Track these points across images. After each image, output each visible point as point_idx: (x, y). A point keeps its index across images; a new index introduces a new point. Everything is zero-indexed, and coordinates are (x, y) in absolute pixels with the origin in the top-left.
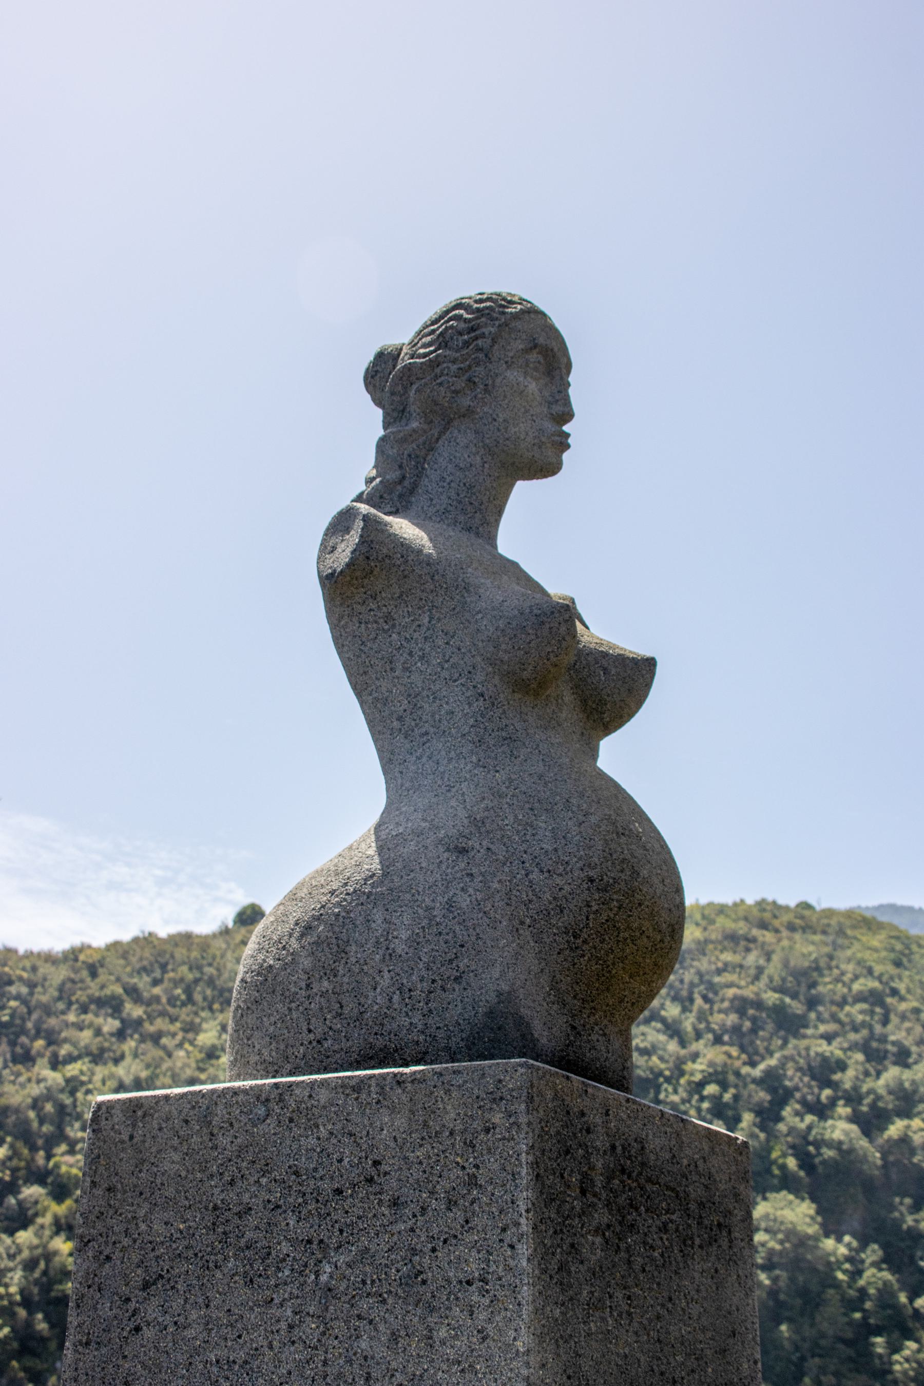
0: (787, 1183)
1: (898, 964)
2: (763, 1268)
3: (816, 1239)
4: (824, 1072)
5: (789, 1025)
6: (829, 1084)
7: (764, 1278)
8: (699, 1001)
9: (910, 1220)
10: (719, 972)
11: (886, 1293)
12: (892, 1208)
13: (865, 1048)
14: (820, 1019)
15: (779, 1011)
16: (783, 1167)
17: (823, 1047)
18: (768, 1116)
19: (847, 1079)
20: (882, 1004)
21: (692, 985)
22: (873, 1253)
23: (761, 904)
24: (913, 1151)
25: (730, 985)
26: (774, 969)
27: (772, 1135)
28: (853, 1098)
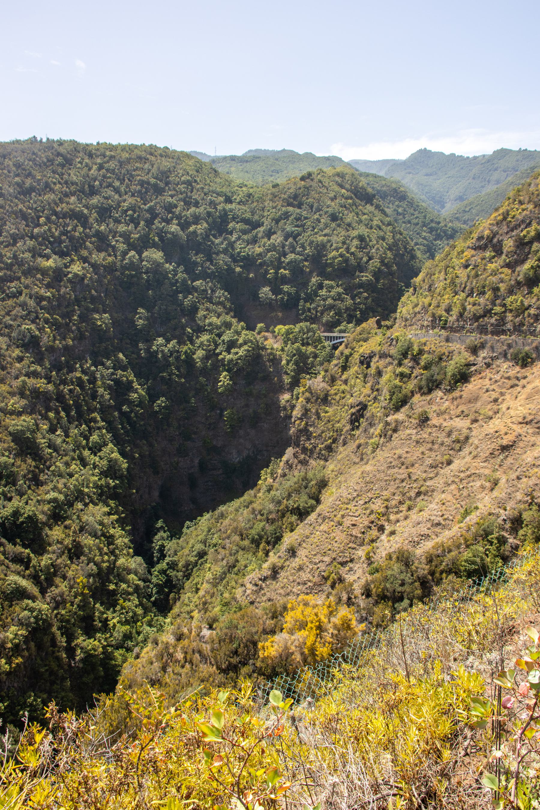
0: (155, 245)
1: (197, 171)
2: (145, 273)
3: (163, 264)
4: (169, 208)
5: (159, 191)
6: (170, 212)
7: (144, 276)
8: (127, 181)
9: (194, 258)
10: (134, 170)
11: (184, 281)
12: (189, 254)
13: (184, 200)
14: (169, 189)
15: (155, 186)
16: (154, 240)
17: (170, 199)
18: (149, 223)
19: (177, 211)
20: (191, 185)
21: (124, 175)
22: (181, 268)
23: (151, 146)
24: (197, 236)
25: (138, 175)
26: (154, 170)
27: (150, 229)
28: (179, 217)
